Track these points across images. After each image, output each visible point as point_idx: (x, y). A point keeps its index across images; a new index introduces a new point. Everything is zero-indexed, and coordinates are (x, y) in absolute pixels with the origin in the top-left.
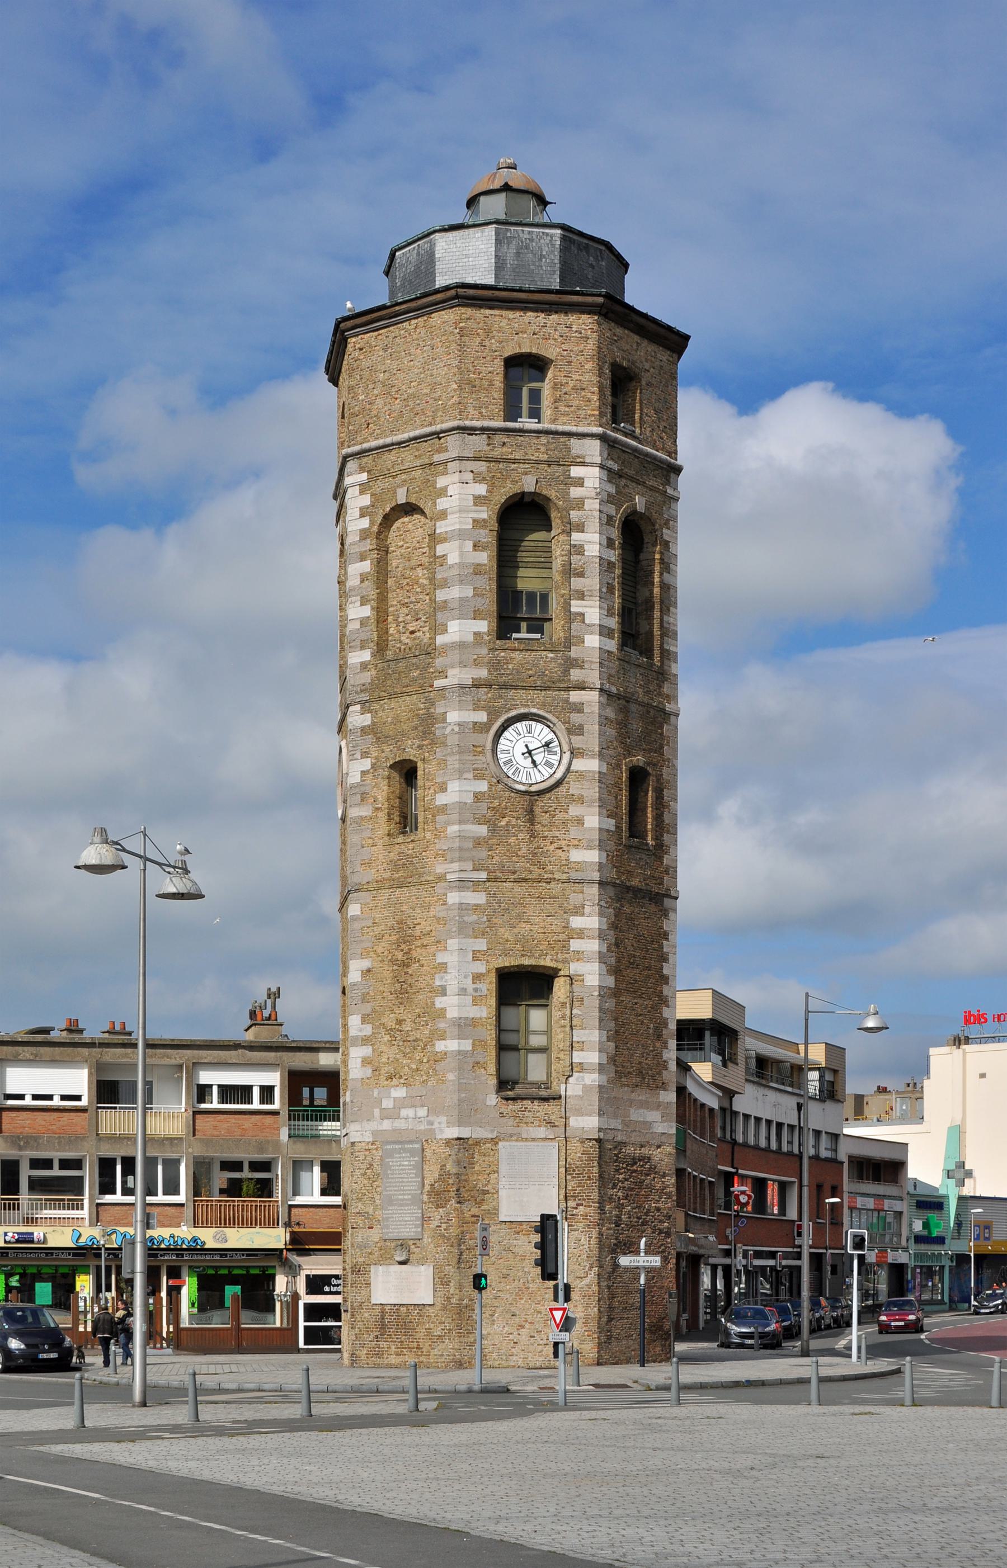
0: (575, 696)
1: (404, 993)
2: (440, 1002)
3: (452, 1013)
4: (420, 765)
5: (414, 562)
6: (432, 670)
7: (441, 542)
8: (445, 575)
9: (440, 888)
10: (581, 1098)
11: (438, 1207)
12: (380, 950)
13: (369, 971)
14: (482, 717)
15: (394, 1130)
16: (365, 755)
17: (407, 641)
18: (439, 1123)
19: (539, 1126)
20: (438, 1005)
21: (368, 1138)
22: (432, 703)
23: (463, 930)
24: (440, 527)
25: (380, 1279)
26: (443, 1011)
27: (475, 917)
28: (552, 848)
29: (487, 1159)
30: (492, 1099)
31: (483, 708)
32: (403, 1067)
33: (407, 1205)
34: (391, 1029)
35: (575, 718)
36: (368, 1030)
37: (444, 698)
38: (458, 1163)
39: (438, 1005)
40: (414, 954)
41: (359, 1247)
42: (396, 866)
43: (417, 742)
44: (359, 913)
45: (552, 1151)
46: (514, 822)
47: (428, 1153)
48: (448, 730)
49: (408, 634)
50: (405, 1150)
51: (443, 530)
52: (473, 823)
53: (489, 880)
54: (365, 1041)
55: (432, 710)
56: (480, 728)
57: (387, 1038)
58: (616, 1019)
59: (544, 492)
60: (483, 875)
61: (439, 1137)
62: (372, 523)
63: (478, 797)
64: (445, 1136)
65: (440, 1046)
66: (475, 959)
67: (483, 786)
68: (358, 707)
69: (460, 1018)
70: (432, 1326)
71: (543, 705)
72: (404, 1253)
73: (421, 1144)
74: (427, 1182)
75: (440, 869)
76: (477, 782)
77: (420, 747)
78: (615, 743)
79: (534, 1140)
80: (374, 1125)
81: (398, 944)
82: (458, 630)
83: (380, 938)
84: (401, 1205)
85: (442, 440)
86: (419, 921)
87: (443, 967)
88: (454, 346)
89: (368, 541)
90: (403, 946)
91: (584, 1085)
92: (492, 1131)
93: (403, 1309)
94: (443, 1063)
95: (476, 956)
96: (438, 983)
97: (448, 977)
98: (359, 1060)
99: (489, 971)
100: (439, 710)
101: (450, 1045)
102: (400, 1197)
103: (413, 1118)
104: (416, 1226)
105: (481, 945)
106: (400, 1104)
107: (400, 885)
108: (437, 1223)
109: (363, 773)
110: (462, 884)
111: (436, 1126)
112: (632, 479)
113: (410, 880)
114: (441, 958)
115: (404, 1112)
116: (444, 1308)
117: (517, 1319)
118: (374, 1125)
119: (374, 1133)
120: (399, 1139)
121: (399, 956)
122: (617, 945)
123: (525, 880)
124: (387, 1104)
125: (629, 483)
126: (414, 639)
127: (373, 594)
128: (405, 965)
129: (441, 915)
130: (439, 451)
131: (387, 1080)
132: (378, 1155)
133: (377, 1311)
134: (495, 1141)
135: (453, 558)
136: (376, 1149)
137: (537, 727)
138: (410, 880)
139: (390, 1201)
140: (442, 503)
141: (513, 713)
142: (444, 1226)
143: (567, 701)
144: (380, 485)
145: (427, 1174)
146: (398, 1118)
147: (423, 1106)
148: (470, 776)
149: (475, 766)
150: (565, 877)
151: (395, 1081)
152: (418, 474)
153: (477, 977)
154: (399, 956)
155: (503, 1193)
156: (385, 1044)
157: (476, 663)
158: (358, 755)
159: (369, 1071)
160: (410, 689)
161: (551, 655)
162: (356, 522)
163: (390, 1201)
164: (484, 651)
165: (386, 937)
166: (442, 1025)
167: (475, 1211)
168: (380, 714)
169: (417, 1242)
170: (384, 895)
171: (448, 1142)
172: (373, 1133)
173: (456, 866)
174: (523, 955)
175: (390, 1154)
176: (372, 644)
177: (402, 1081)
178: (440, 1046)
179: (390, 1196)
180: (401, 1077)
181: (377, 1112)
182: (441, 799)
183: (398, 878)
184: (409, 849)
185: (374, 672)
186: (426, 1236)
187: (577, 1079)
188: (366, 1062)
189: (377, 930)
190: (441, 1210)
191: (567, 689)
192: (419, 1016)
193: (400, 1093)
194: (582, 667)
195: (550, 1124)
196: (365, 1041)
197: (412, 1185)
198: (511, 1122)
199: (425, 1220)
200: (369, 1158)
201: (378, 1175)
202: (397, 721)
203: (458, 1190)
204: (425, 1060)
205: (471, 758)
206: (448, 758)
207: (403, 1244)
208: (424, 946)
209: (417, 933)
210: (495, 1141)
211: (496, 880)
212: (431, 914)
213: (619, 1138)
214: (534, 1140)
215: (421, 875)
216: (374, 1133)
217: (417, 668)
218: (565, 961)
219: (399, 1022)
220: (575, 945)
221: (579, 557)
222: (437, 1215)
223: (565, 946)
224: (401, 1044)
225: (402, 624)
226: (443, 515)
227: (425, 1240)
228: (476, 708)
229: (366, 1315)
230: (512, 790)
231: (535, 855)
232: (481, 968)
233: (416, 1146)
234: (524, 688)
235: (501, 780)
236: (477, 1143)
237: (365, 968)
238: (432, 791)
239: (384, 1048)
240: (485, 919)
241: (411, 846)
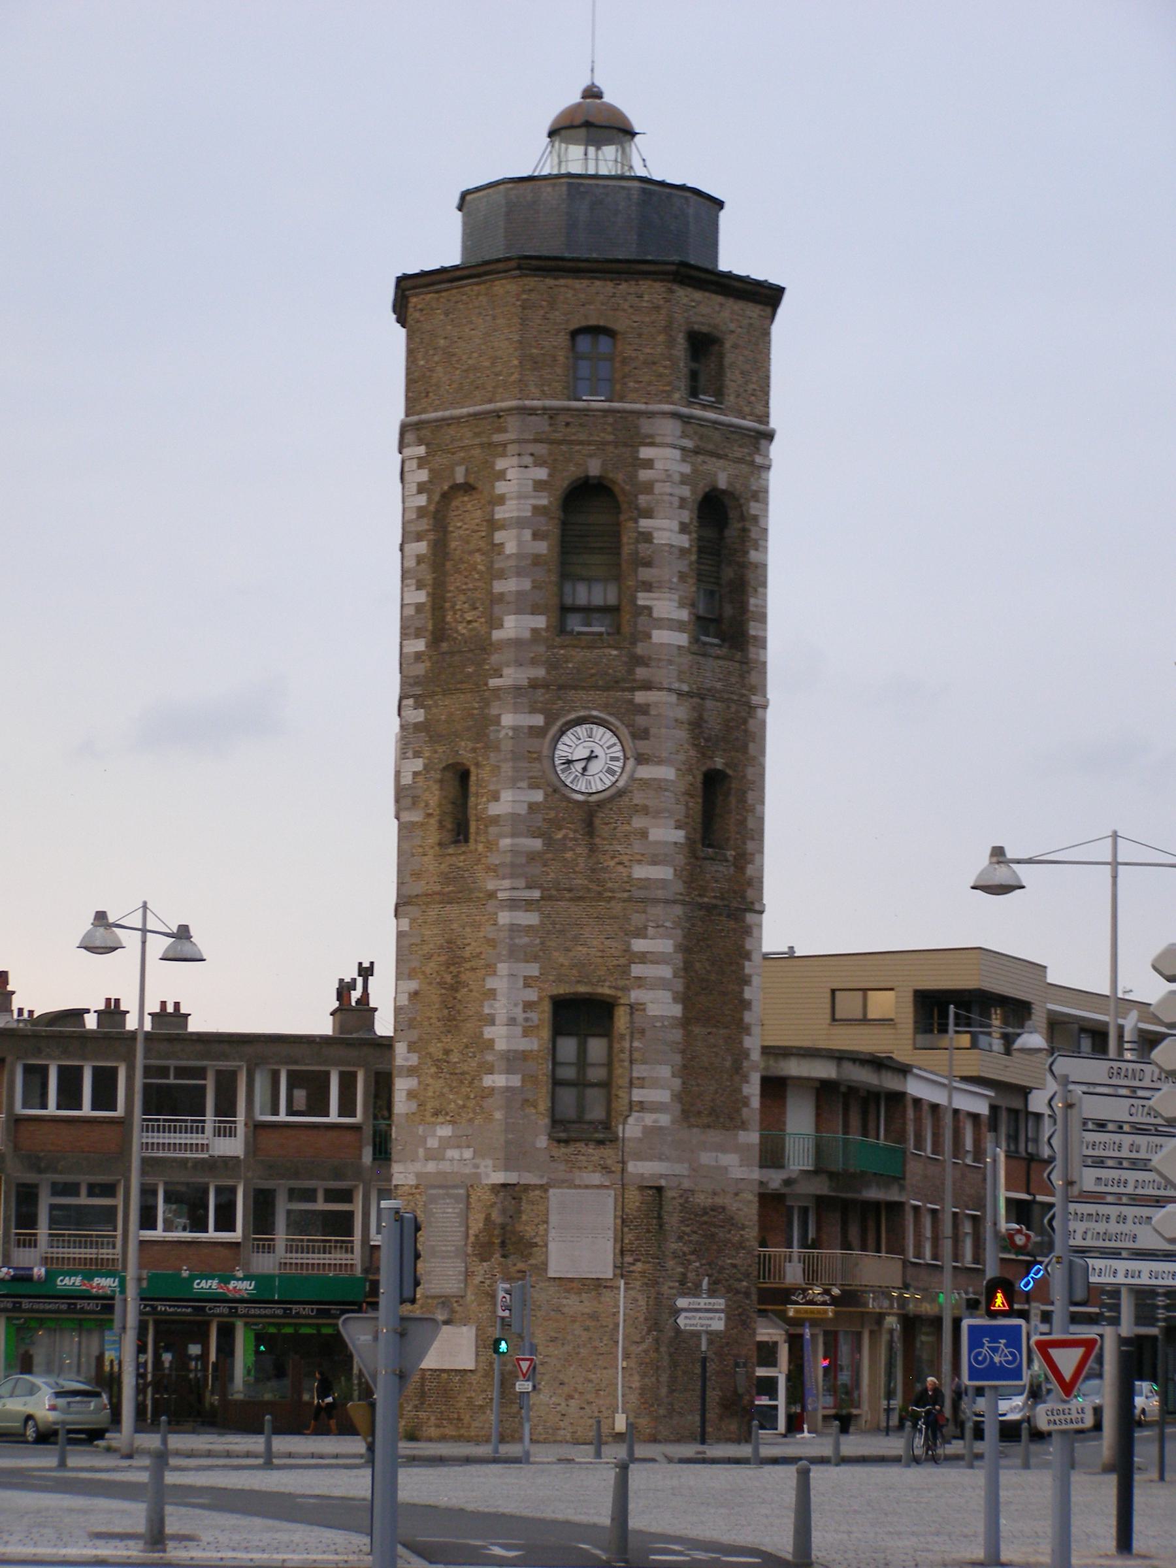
0: (640, 697)
1: (452, 1019)
2: (489, 1032)
3: (501, 1045)
4: (473, 769)
5: (472, 547)
7: (499, 529)
9: (491, 906)
10: (640, 1140)
11: (483, 1260)
12: (428, 971)
13: (416, 993)
14: (538, 720)
15: (439, 1173)
16: (417, 754)
17: (464, 631)
18: (486, 1167)
19: (593, 1172)
20: (487, 1036)
21: (412, 1181)
22: (486, 703)
23: (514, 954)
26: (492, 1041)
27: (526, 940)
28: (612, 863)
29: (535, 1207)
30: (542, 1142)
31: (540, 711)
32: (449, 1104)
33: (450, 1257)
35: (641, 721)
36: (414, 1059)
37: (499, 698)
38: (504, 1211)
39: (487, 1036)
40: (463, 977)
42: (446, 879)
43: (470, 745)
44: (407, 929)
45: (609, 1199)
46: (571, 835)
48: (502, 734)
49: (464, 624)
50: (449, 1196)
52: (527, 837)
53: (542, 898)
54: (412, 1071)
56: (537, 732)
57: (433, 1070)
58: (683, 1052)
59: (611, 475)
60: (536, 894)
61: (485, 1182)
62: (429, 500)
63: (533, 807)
64: (491, 1181)
65: (488, 1081)
66: (527, 985)
67: (538, 796)
69: (509, 1051)
70: (473, 1394)
71: (605, 707)
74: (471, 1232)
75: (491, 886)
76: (533, 792)
77: (474, 750)
78: (686, 746)
79: (587, 1187)
80: (418, 1167)
81: (448, 965)
82: (513, 626)
83: (428, 957)
84: (443, 1258)
87: (492, 994)
89: (425, 520)
90: (452, 968)
91: (645, 1127)
92: (542, 1177)
93: (444, 1376)
94: (490, 1100)
95: (528, 982)
96: (487, 1011)
97: (497, 1005)
99: (541, 999)
100: (494, 711)
101: (498, 1080)
103: (459, 1159)
105: (533, 970)
106: (445, 1143)
107: (447, 899)
108: (480, 1279)
109: (415, 774)
110: (513, 904)
111: (482, 1170)
112: (713, 454)
113: (460, 895)
114: (491, 983)
117: (566, 1389)
119: (418, 1175)
120: (444, 1184)
121: (448, 979)
122: (686, 969)
123: (581, 898)
124: (432, 1143)
125: (707, 459)
126: (471, 630)
127: (429, 578)
128: (454, 988)
129: (491, 936)
134: (544, 1188)
135: (511, 548)
136: (420, 1194)
137: (599, 731)
138: (460, 895)
141: (573, 716)
142: (488, 1282)
143: (631, 702)
145: (471, 1223)
146: (443, 1159)
147: (469, 1147)
148: (524, 784)
149: (531, 774)
150: (626, 895)
151: (441, 1119)
152: (477, 452)
153: (528, 1006)
154: (448, 979)
155: (552, 1246)
156: (432, 1077)
157: (534, 662)
159: (413, 1106)
160: (464, 686)
161: (615, 652)
164: (542, 649)
165: (435, 958)
166: (490, 1058)
167: (521, 1266)
168: (434, 710)
170: (433, 912)
173: (507, 883)
174: (578, 982)
177: (448, 1118)
178: (488, 1081)
180: (447, 1114)
181: (421, 1151)
182: (495, 809)
183: (450, 892)
184: (460, 861)
185: (428, 664)
186: (469, 1293)
187: (637, 1120)
188: (411, 1095)
189: (426, 949)
191: (632, 690)
193: (445, 1131)
194: (647, 665)
195: (606, 1169)
196: (412, 1071)
198: (562, 1167)
199: (468, 1274)
205: (527, 765)
208: (473, 969)
209: (467, 954)
210: (544, 1188)
211: (550, 898)
212: (481, 934)
213: (686, 1184)
214: (587, 1187)
216: (418, 1175)
218: (626, 989)
219: (447, 1052)
220: (637, 970)
221: (647, 545)
223: (625, 971)
228: (533, 710)
230: (569, 800)
231: (593, 871)
232: (532, 995)
233: (462, 1191)
234: (584, 688)
235: (557, 790)
236: (527, 1188)
237: (412, 990)
238: (484, 799)
239: (430, 1081)
240: (538, 941)
241: (462, 858)
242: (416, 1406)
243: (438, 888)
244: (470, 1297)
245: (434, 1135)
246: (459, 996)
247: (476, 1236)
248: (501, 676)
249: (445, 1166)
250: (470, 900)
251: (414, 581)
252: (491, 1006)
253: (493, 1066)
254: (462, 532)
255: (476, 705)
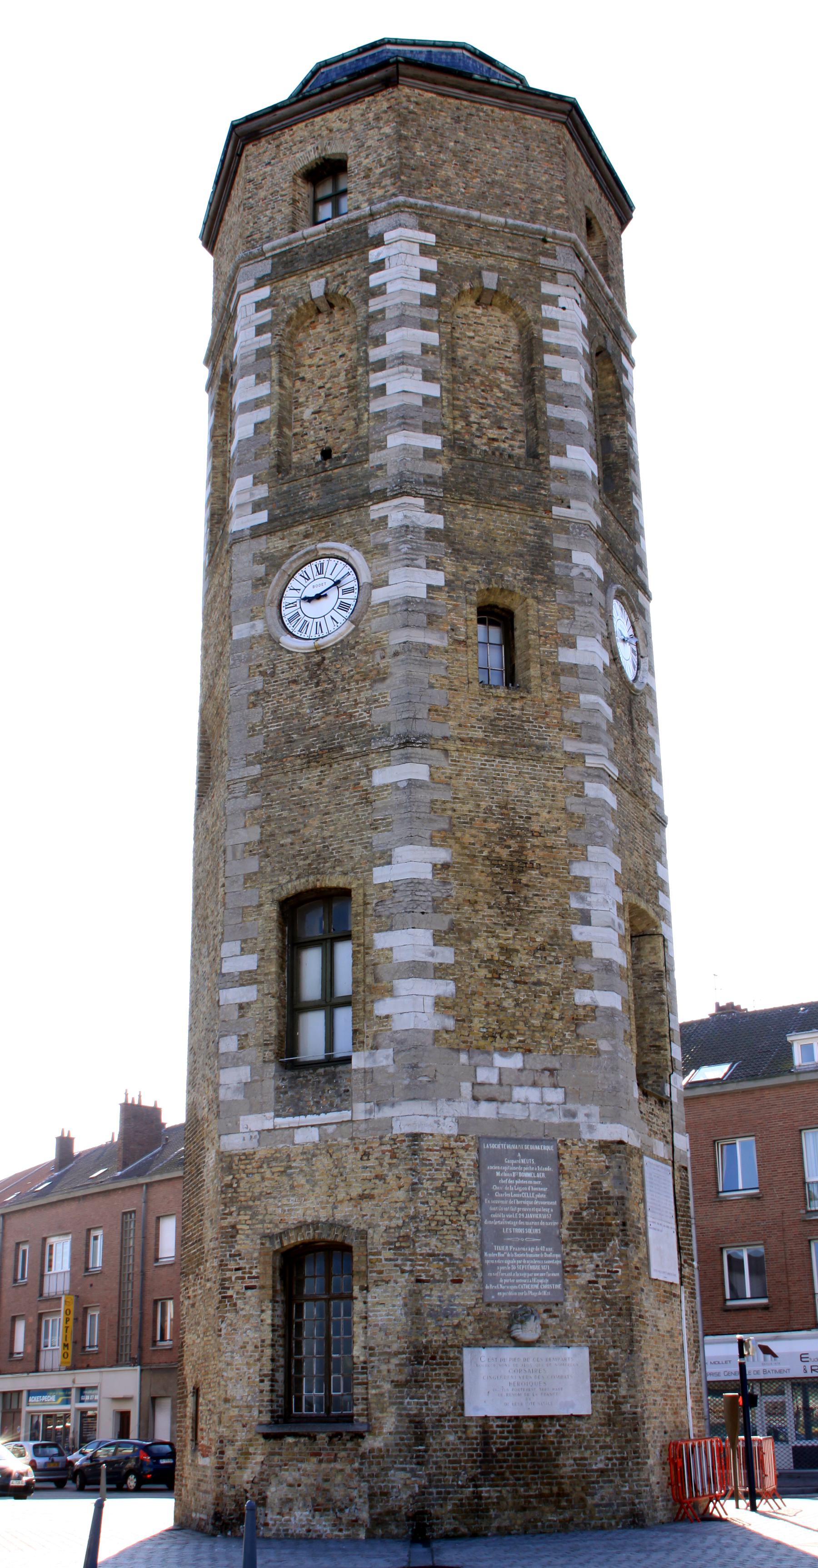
2: (580, 933)
6: (543, 492)
8: (560, 391)
9: (573, 773)
11: (589, 1249)
13: (446, 866)
15: (501, 1121)
16: (432, 565)
18: (587, 1115)
21: (450, 1128)
24: (549, 336)
25: (483, 1371)
33: (533, 1244)
34: (491, 960)
36: (446, 955)
37: (566, 531)
41: (433, 1314)
43: (523, 574)
47: (567, 1161)
48: (575, 572)
50: (526, 1154)
51: (552, 340)
55: (548, 541)
57: (483, 972)
61: (586, 1136)
65: (583, 997)
68: (421, 502)
70: (587, 1454)
72: (504, 1324)
73: (554, 1149)
74: (567, 1209)
80: (464, 1108)
85: (547, 246)
86: (535, 810)
87: (582, 884)
88: (556, 159)
90: (511, 842)
96: (574, 904)
97: (592, 898)
98: (429, 1002)
102: (520, 1231)
103: (535, 1103)
104: (552, 1281)
108: (589, 1276)
109: (430, 588)
111: (581, 1118)
113: (523, 750)
115: (519, 1093)
116: (610, 1421)
118: (464, 1108)
120: (518, 1137)
130: (545, 254)
131: (484, 1038)
132: (468, 1159)
133: (474, 1431)
136: (466, 1148)
139: (499, 1237)
140: (548, 311)
142: (602, 1282)
144: (454, 256)
145: (566, 1194)
146: (510, 1101)
147: (555, 1086)
151: (499, 1043)
154: (504, 853)
158: (422, 562)
162: (415, 283)
163: (499, 1237)
166: (585, 967)
168: (459, 520)
169: (554, 1308)
171: (605, 1147)
172: (459, 1120)
175: (499, 1158)
176: (444, 432)
177: (513, 1042)
178: (583, 997)
179: (499, 1228)
180: (511, 1037)
181: (466, 1088)
185: (447, 467)
186: (570, 1298)
188: (440, 1004)
190: (595, 1255)
192: (543, 949)
197: (540, 1212)
199: (568, 1269)
200: (451, 1163)
201: (471, 1192)
202: (488, 537)
203: (624, 1224)
204: (556, 1015)
206: (576, 606)
207: (521, 1312)
209: (535, 826)
215: (540, 748)
216: (459, 1120)
217: (520, 483)
222: (588, 1266)
224: (510, 985)
225: (475, 426)
226: (553, 324)
227: (568, 1305)
229: (451, 1438)
241: (517, 705)
242: (473, 1479)
243: (480, 734)
244: (570, 1305)
245: (491, 1065)
246: (524, 880)
247: (576, 1215)
248: (569, 507)
249: (507, 1110)
250: (538, 759)
251: (420, 370)
252: (583, 899)
253: (591, 978)
254: (473, 343)
255: (531, 531)
